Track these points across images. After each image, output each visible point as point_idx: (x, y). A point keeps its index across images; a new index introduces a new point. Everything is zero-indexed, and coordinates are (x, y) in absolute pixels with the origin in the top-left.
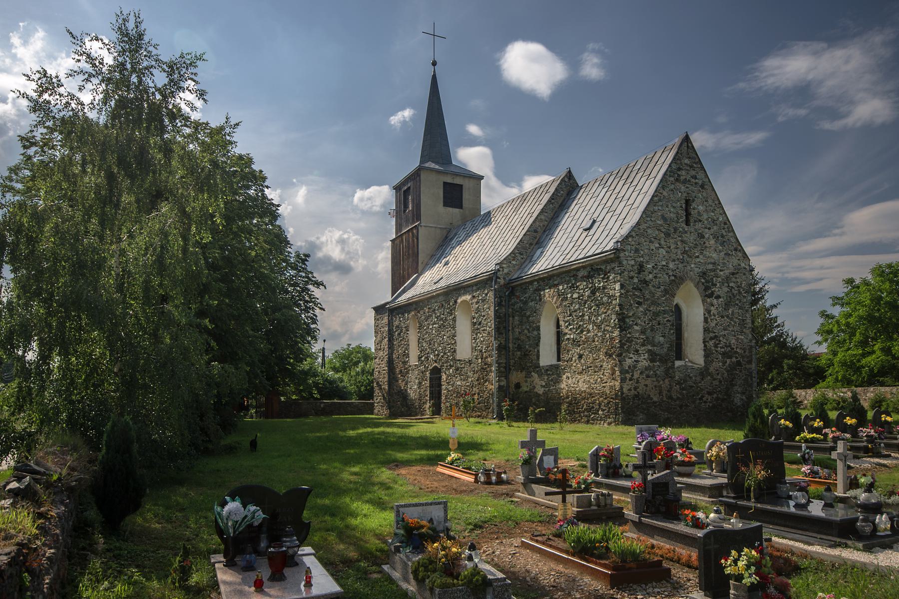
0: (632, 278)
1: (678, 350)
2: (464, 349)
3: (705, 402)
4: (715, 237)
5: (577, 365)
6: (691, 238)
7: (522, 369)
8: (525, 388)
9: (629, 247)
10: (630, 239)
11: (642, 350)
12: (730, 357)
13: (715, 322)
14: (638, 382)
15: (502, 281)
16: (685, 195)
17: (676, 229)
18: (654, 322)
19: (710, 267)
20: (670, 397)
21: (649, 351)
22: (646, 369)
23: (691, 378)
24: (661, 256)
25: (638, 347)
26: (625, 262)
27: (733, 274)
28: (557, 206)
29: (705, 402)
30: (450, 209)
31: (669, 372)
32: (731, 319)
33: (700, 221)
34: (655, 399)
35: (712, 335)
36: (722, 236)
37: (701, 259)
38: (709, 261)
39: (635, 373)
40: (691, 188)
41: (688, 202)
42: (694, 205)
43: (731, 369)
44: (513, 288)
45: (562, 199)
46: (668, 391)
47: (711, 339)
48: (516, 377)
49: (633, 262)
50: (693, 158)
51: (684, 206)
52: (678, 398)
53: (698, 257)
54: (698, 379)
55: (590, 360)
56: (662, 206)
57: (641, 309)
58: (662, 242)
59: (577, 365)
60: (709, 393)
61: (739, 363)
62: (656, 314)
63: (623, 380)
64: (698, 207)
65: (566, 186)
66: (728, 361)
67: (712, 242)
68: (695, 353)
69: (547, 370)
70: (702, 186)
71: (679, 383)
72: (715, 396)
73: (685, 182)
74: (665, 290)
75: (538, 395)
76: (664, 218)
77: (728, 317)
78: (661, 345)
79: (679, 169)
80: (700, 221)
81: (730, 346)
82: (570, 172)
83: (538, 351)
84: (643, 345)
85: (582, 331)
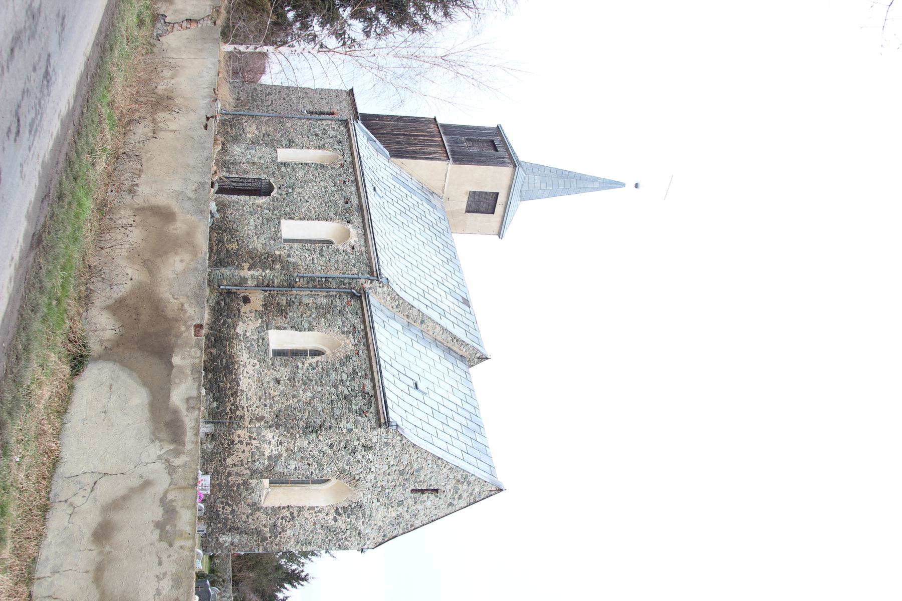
1: (280, 481)
3: (223, 508)
5: (269, 376)
6: (398, 495)
7: (265, 306)
8: (244, 308)
9: (390, 436)
10: (399, 438)
13: (309, 517)
14: (247, 444)
15: (367, 285)
16: (443, 489)
18: (311, 460)
19: (367, 512)
20: (230, 474)
21: (280, 455)
24: (381, 467)
26: (375, 433)
27: (359, 534)
28: (449, 345)
29: (223, 508)
30: (466, 199)
32: (312, 532)
33: (416, 503)
35: (296, 514)
36: (399, 523)
38: (374, 511)
40: (450, 494)
41: (437, 491)
42: (432, 496)
43: (258, 532)
44: (360, 297)
45: (457, 350)
47: (292, 514)
48: (257, 299)
49: (375, 440)
51: (432, 488)
53: (378, 500)
54: (249, 501)
55: (273, 393)
58: (394, 468)
59: (269, 376)
60: (233, 511)
61: (264, 539)
62: (320, 464)
64: (429, 500)
65: (471, 355)
67: (394, 514)
69: (263, 339)
70: (450, 504)
72: (230, 517)
73: (456, 490)
74: (344, 470)
76: (418, 470)
77: (314, 529)
80: (416, 503)
81: (283, 531)
82: (487, 358)
83: (285, 328)
84: (287, 449)
85: (305, 384)
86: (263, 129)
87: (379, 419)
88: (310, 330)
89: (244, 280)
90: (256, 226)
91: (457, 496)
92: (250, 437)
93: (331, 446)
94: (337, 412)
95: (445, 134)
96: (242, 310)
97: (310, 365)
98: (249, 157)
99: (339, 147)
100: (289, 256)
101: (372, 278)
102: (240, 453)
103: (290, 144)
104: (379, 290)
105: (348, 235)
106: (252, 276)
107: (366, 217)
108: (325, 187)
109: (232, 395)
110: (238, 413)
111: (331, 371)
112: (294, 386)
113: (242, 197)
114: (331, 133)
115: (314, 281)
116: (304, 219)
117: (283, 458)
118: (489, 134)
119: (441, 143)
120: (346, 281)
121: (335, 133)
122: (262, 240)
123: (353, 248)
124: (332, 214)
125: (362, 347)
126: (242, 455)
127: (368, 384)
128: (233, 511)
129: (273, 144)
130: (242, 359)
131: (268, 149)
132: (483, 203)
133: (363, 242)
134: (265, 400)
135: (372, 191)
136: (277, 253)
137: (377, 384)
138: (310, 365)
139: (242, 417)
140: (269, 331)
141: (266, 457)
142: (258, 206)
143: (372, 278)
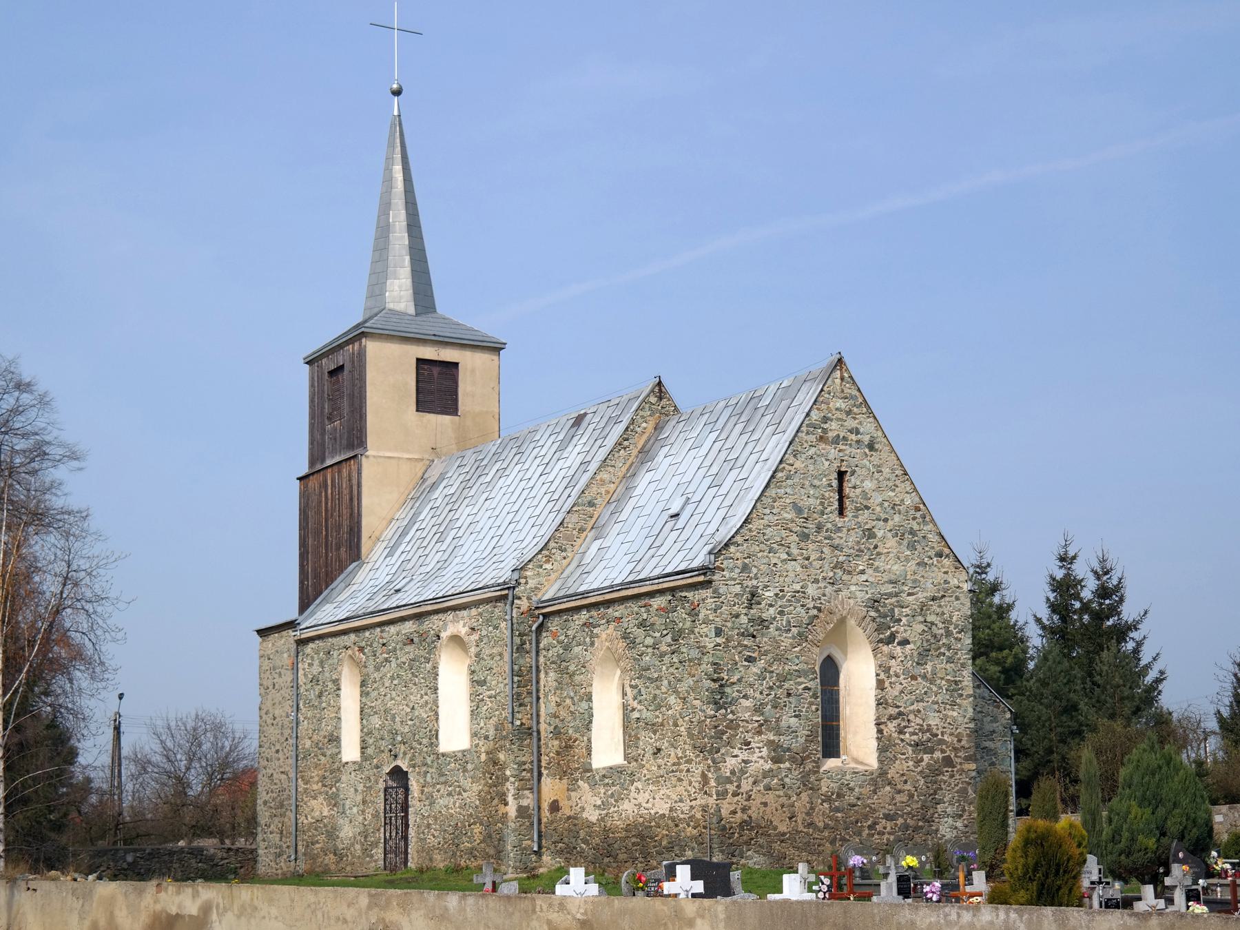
0: (737, 616)
2: (455, 732)
4: (898, 533)
6: (850, 540)
8: (566, 811)
10: (732, 549)
11: (756, 742)
12: (931, 751)
14: (749, 798)
15: (524, 604)
17: (819, 528)
19: (889, 589)
21: (770, 743)
22: (766, 774)
23: (852, 789)
24: (792, 574)
25: (748, 737)
28: (635, 452)
29: (881, 833)
31: (808, 783)
33: (867, 508)
34: (783, 828)
35: (893, 711)
37: (870, 575)
39: (744, 782)
40: (848, 450)
41: (841, 475)
43: (934, 772)
44: (545, 616)
46: (808, 814)
47: (891, 718)
49: (738, 589)
50: (852, 397)
51: (835, 483)
52: (826, 827)
53: (863, 572)
54: (867, 790)
55: (673, 759)
56: (792, 486)
57: (755, 670)
58: (795, 551)
60: (888, 817)
61: (948, 761)
62: (783, 678)
63: (722, 795)
64: (861, 484)
66: (926, 757)
67: (892, 542)
68: (861, 743)
69: (604, 776)
70: (871, 447)
71: (828, 799)
72: (900, 821)
73: (836, 441)
74: (800, 634)
75: (590, 825)
76: (798, 510)
77: (924, 677)
78: (791, 731)
79: (825, 420)
80: (867, 508)
81: (929, 730)
82: (660, 383)
83: (589, 740)
84: (759, 733)
85: (659, 707)
86: (315, 787)
87: (701, 583)
88: (590, 700)
89: (522, 811)
90: (450, 794)
91: (853, 437)
92: (735, 794)
93: (750, 659)
94: (695, 653)
95: (323, 461)
96: (568, 812)
97: (635, 699)
98: (355, 810)
99: (335, 653)
100: (486, 738)
101: (510, 598)
102: (768, 809)
103: (335, 740)
104: (532, 583)
105: (456, 639)
106: (517, 797)
107: (429, 608)
108: (392, 678)
109: (677, 826)
110: (698, 815)
111: (642, 664)
112: (662, 725)
113: (411, 822)
114: (316, 669)
115: (519, 694)
116: (437, 714)
117: (776, 738)
118: (320, 379)
119: (335, 468)
120: (517, 640)
121: (316, 663)
122: (467, 783)
123: (473, 629)
124: (429, 666)
125: (610, 610)
126: (773, 805)
127: (657, 602)
128: (888, 817)
129: (336, 768)
130: (630, 812)
131: (344, 778)
132: (437, 388)
133: (465, 613)
134: (681, 771)
135: (399, 595)
136: (483, 757)
137: (655, 587)
138: (635, 699)
139: (704, 809)
140: (594, 766)
141: (775, 767)
142: (422, 792)
143: (510, 598)
